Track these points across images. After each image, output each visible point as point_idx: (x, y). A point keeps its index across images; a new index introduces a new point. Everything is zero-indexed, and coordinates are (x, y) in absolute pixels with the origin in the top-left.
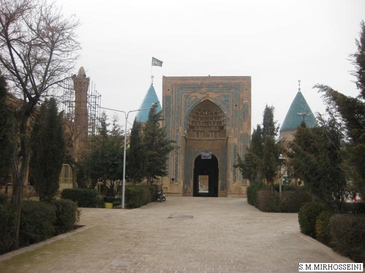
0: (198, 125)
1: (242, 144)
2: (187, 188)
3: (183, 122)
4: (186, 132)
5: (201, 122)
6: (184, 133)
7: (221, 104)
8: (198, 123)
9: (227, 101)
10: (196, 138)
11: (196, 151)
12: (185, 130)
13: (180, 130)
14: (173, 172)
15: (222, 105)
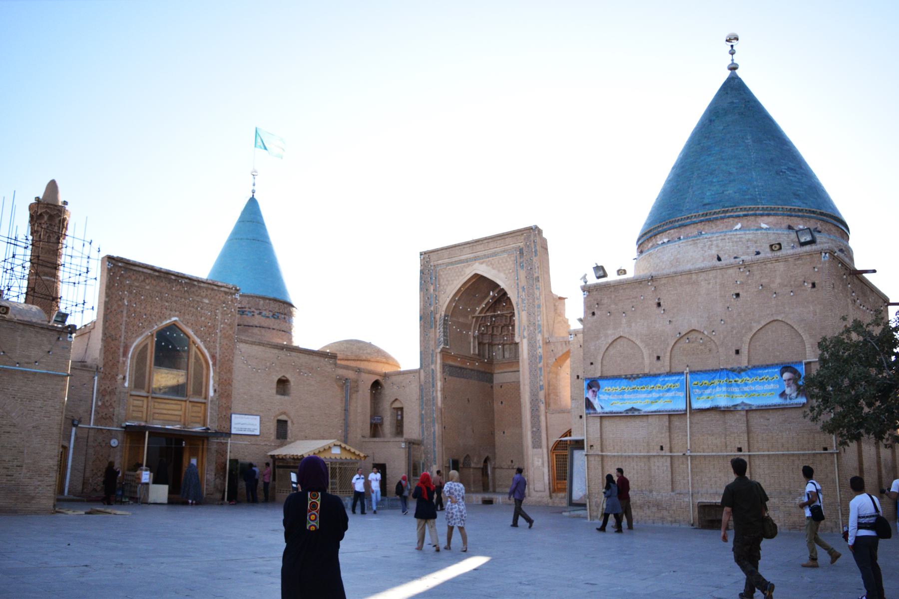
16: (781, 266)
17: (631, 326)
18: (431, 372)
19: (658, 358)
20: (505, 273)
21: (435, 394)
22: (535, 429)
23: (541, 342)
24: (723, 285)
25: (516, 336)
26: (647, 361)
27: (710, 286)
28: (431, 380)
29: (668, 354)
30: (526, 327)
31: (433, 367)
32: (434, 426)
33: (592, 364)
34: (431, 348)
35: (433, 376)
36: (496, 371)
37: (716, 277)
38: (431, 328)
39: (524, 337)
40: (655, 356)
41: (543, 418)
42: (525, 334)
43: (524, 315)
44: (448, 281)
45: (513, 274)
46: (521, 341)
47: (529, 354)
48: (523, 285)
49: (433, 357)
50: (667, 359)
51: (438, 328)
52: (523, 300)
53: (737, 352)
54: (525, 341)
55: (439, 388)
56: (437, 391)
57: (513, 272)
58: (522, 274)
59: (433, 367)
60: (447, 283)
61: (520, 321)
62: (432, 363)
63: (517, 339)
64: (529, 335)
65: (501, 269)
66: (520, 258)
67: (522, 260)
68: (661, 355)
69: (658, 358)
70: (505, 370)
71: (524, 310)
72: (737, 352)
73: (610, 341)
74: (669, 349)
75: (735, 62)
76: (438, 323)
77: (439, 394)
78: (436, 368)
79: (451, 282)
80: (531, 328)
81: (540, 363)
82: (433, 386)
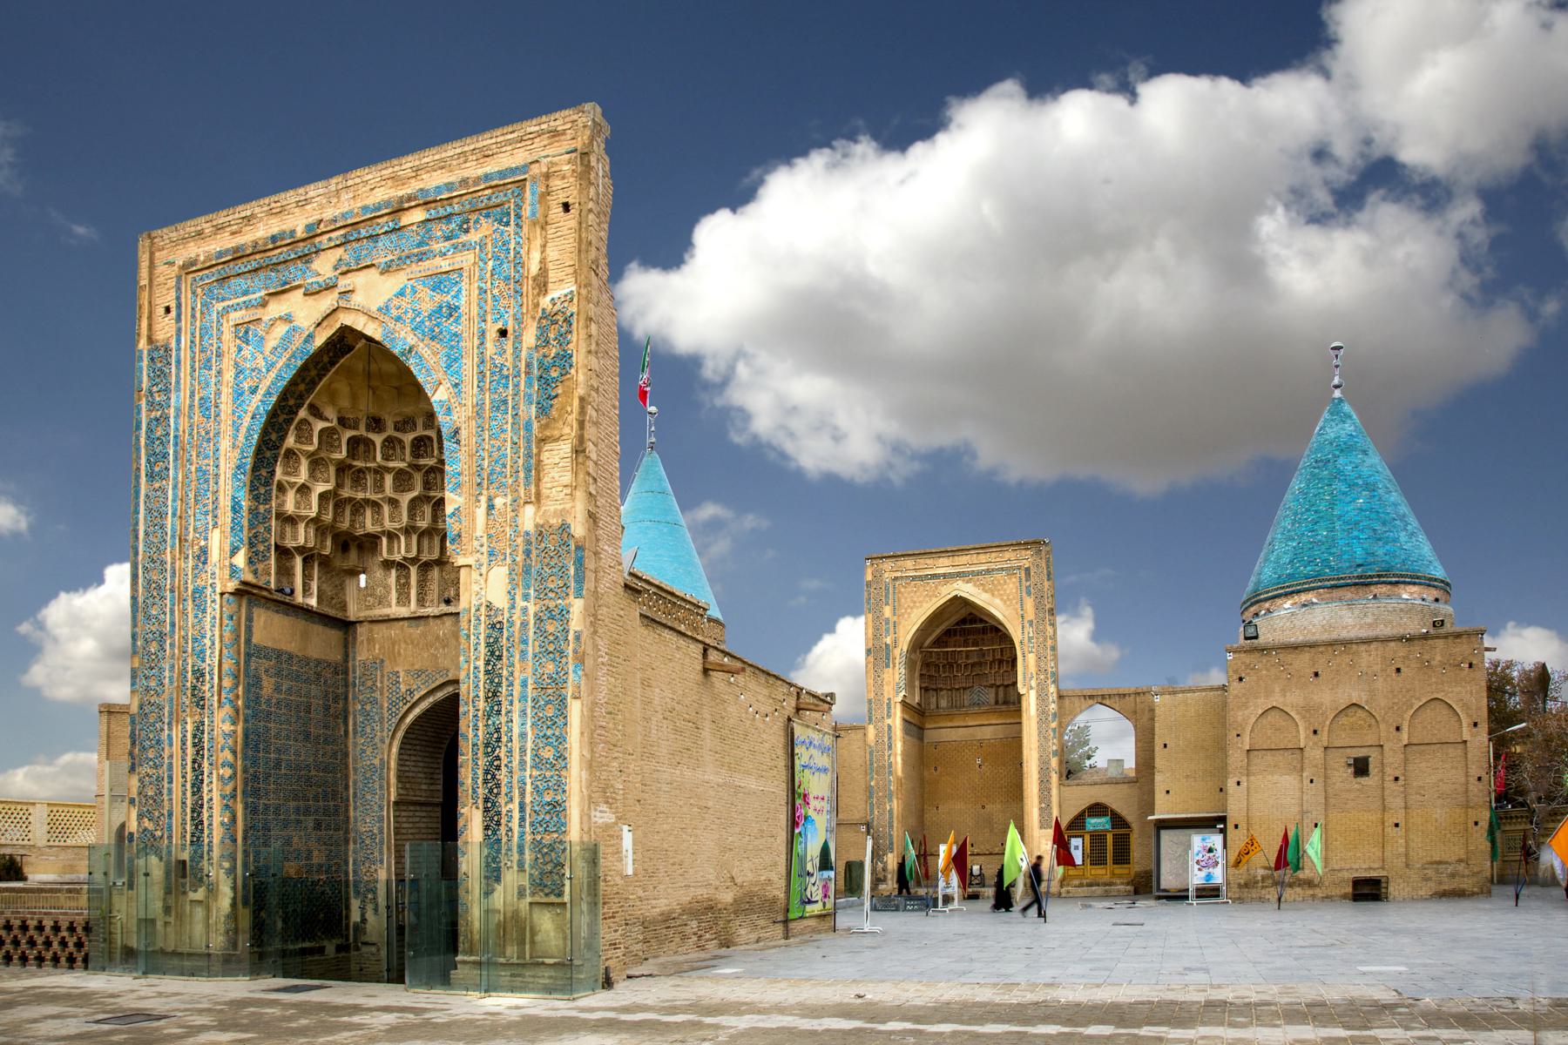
0: (388, 525)
1: (532, 609)
2: (364, 920)
3: (225, 502)
4: (240, 560)
5: (405, 499)
6: (234, 570)
7: (411, 340)
8: (386, 509)
9: (453, 310)
10: (396, 610)
11: (403, 688)
12: (234, 551)
13: (214, 555)
14: (184, 823)
15: (423, 350)
16: (1440, 643)
17: (1285, 696)
18: (886, 729)
19: (1315, 732)
20: (1002, 600)
21: (892, 759)
22: (1043, 805)
24: (1384, 658)
25: (1020, 685)
26: (1302, 736)
27: (1371, 658)
28: (886, 740)
29: (1326, 729)
30: (1034, 675)
31: (889, 721)
32: (891, 800)
33: (1238, 735)
34: (886, 696)
35: (889, 734)
36: (928, 726)
37: (1377, 649)
38: (888, 666)
39: (1032, 688)
40: (1312, 729)
41: (1054, 792)
42: (1033, 683)
43: (1031, 658)
44: (915, 602)
48: (1030, 618)
49: (889, 708)
50: (1326, 733)
51: (897, 668)
52: (1030, 639)
54: (1033, 694)
55: (899, 752)
56: (896, 755)
57: (1014, 598)
59: (889, 721)
60: (912, 605)
61: (1026, 667)
62: (889, 717)
63: (1021, 689)
64: (1038, 684)
66: (1027, 581)
67: (1028, 584)
68: (1319, 729)
69: (1315, 732)
70: (970, 724)
71: (1032, 652)
72: (1398, 729)
73: (1260, 712)
74: (1328, 723)
76: (897, 661)
77: (899, 759)
78: (894, 721)
79: (918, 604)
80: (1042, 677)
82: (890, 747)
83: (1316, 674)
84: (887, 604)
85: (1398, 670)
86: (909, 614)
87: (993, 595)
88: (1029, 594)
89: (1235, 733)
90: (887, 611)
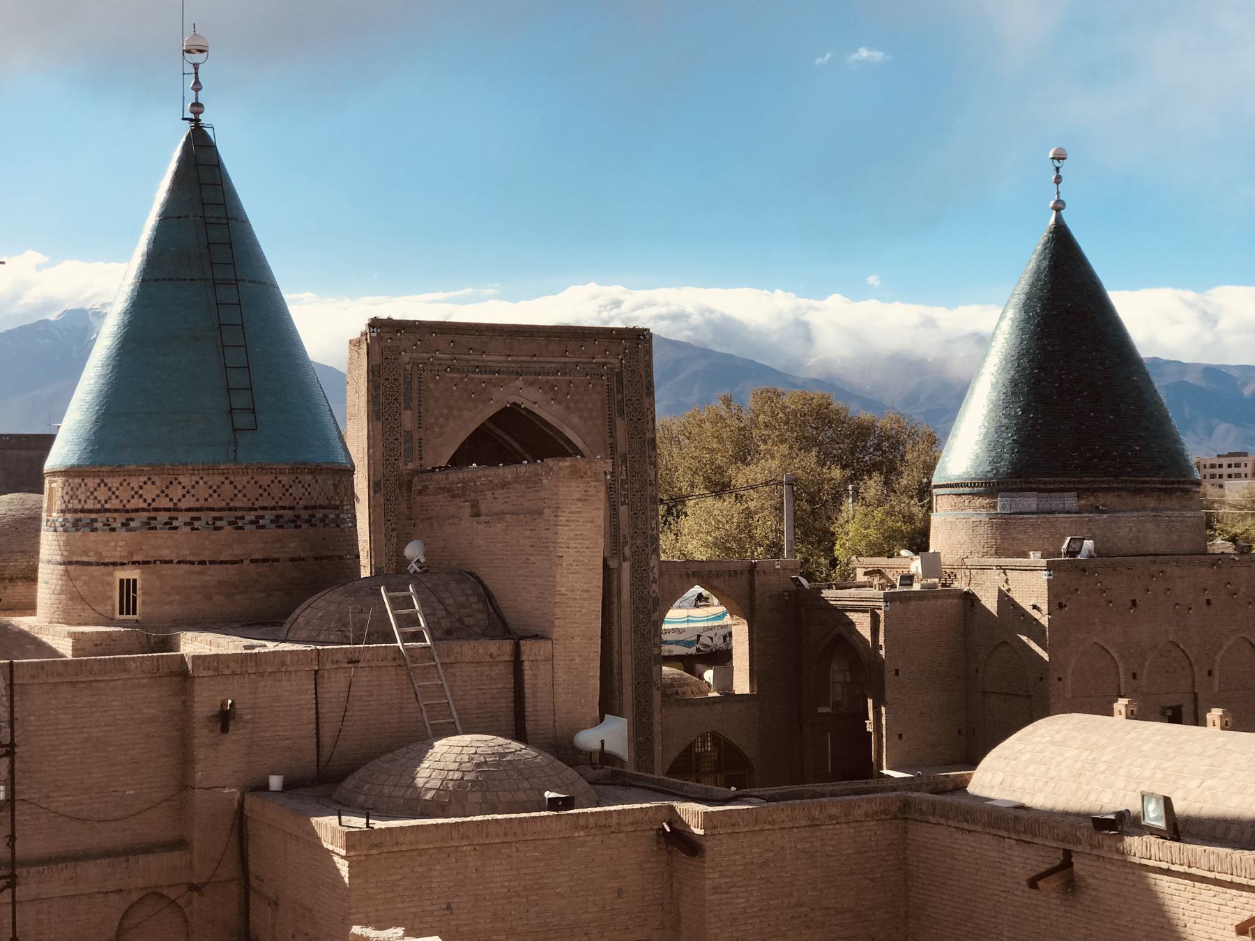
19: (1134, 676)
23: (656, 570)
33: (1060, 679)
39: (625, 559)
42: (627, 551)
45: (599, 422)
46: (620, 565)
47: (632, 593)
53: (1210, 673)
54: (626, 566)
58: (621, 426)
60: (445, 411)
64: (633, 554)
65: (572, 405)
69: (1134, 676)
75: (1061, 198)
79: (456, 412)
81: (654, 612)
83: (1134, 603)
84: (408, 407)
85: (1208, 602)
86: (442, 427)
87: (568, 408)
88: (622, 414)
89: (1056, 677)
90: (408, 419)
